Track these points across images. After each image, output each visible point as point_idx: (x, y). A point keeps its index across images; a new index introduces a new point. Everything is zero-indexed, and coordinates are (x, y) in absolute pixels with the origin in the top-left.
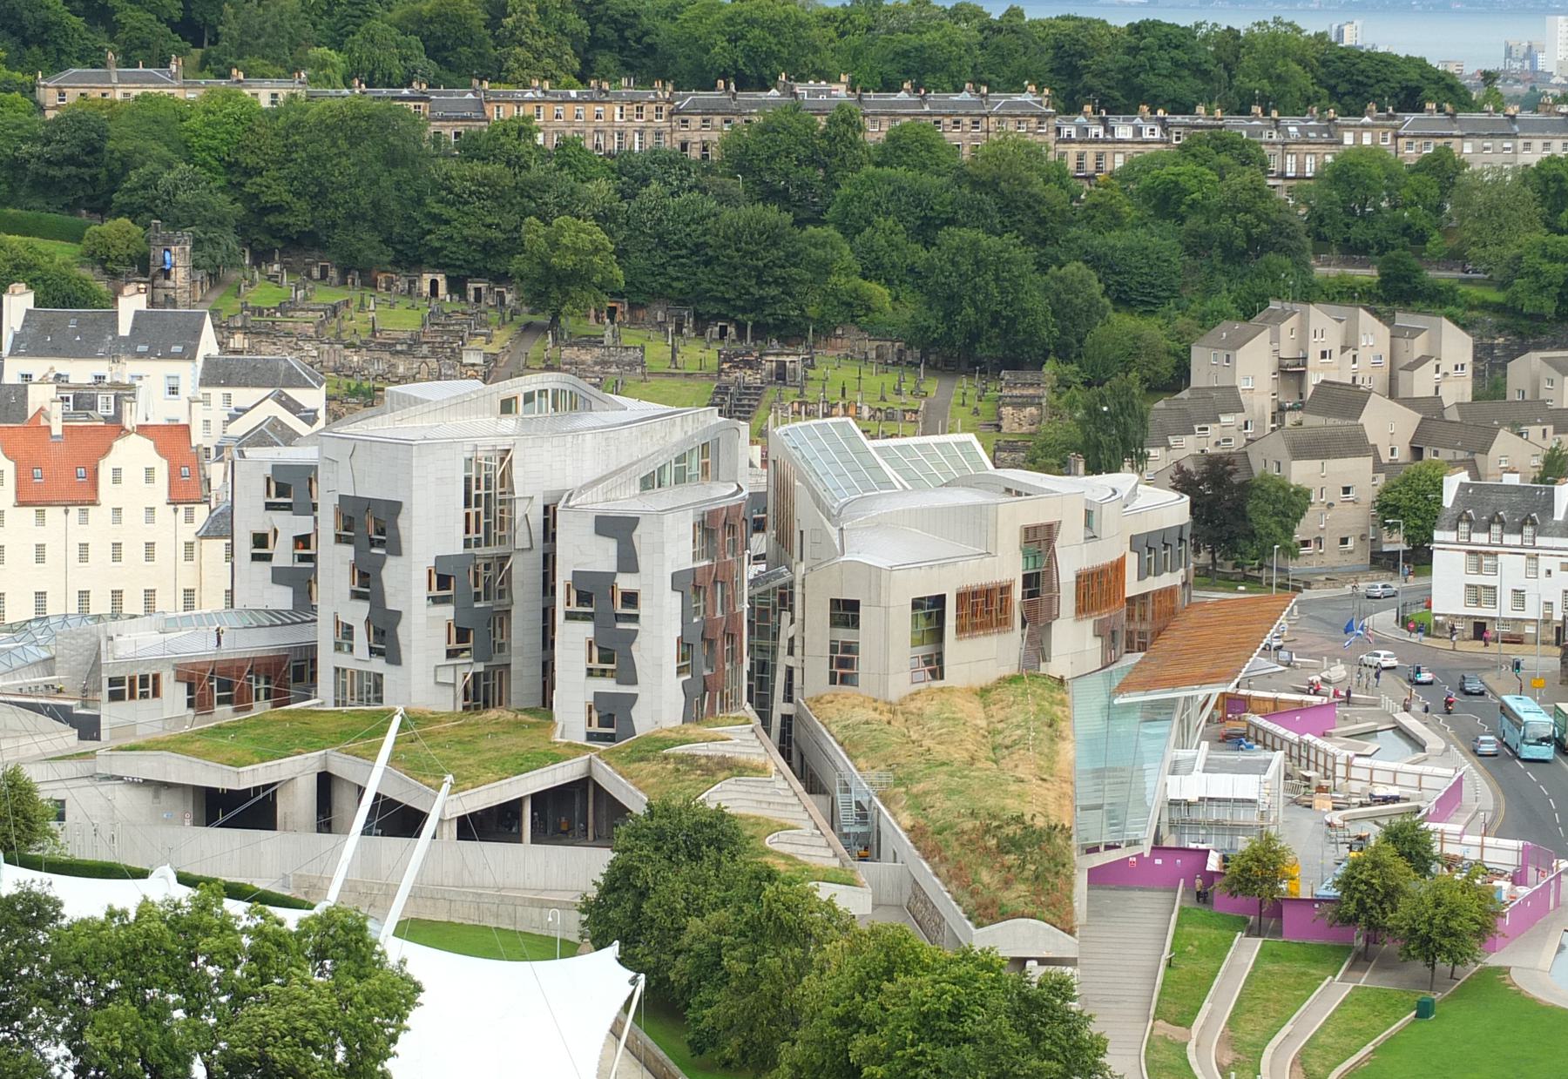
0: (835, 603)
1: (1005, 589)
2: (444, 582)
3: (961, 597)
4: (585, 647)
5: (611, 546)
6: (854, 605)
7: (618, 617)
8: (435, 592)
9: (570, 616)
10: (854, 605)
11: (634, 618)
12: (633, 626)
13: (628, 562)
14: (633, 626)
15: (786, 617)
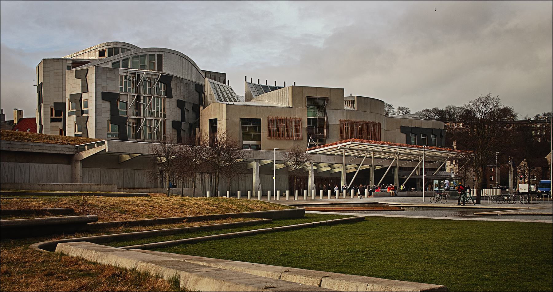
0: (210, 121)
1: (298, 122)
2: (58, 113)
3: (271, 122)
4: (73, 125)
5: (80, 81)
6: (216, 120)
7: (83, 112)
8: (54, 117)
9: (70, 114)
10: (216, 120)
11: (87, 112)
12: (86, 115)
13: (85, 89)
14: (86, 115)
15: (197, 129)
